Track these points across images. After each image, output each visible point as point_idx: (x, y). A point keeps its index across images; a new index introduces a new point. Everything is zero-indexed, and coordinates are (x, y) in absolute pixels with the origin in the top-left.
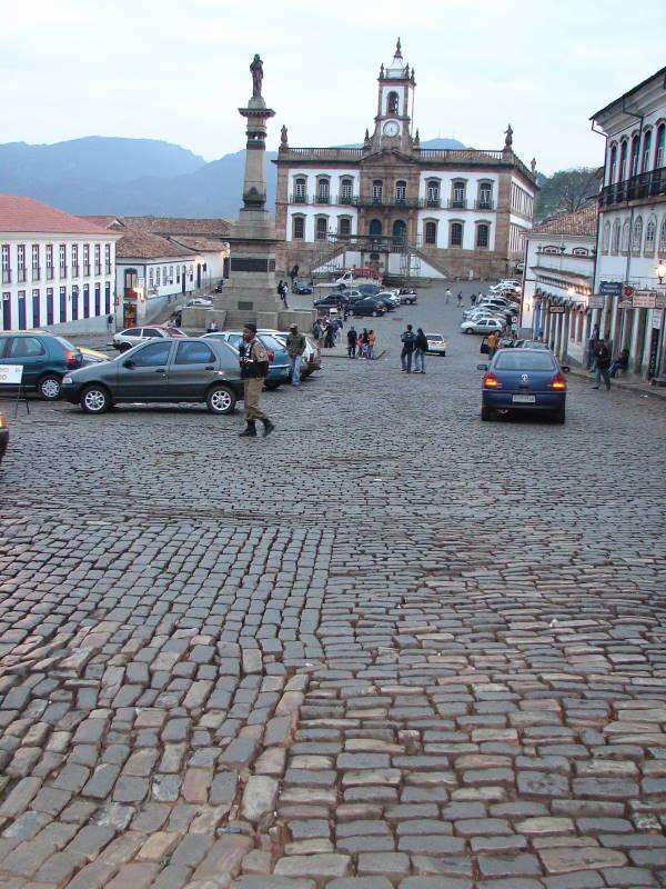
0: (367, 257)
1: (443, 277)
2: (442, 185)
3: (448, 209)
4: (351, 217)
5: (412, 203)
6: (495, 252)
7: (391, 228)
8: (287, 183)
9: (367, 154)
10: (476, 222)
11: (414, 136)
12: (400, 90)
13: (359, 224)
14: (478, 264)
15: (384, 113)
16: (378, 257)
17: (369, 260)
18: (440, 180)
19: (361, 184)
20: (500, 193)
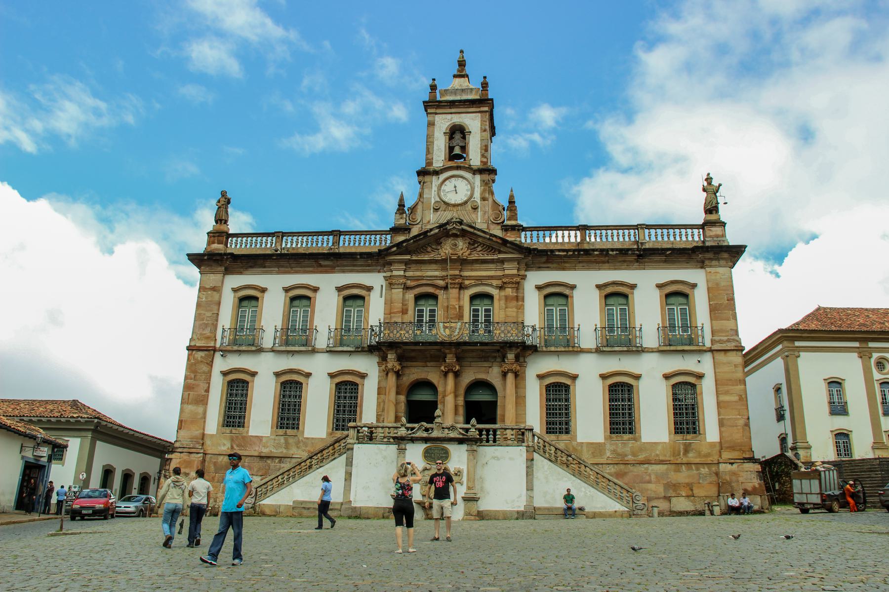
2: (577, 297)
3: (598, 351)
5: (513, 336)
6: (722, 446)
7: (461, 401)
8: (219, 304)
9: (401, 238)
10: (667, 377)
11: (506, 205)
12: (473, 122)
13: (381, 391)
14: (683, 476)
15: (439, 159)
16: (445, 455)
18: (573, 287)
19: (389, 303)
20: (714, 310)
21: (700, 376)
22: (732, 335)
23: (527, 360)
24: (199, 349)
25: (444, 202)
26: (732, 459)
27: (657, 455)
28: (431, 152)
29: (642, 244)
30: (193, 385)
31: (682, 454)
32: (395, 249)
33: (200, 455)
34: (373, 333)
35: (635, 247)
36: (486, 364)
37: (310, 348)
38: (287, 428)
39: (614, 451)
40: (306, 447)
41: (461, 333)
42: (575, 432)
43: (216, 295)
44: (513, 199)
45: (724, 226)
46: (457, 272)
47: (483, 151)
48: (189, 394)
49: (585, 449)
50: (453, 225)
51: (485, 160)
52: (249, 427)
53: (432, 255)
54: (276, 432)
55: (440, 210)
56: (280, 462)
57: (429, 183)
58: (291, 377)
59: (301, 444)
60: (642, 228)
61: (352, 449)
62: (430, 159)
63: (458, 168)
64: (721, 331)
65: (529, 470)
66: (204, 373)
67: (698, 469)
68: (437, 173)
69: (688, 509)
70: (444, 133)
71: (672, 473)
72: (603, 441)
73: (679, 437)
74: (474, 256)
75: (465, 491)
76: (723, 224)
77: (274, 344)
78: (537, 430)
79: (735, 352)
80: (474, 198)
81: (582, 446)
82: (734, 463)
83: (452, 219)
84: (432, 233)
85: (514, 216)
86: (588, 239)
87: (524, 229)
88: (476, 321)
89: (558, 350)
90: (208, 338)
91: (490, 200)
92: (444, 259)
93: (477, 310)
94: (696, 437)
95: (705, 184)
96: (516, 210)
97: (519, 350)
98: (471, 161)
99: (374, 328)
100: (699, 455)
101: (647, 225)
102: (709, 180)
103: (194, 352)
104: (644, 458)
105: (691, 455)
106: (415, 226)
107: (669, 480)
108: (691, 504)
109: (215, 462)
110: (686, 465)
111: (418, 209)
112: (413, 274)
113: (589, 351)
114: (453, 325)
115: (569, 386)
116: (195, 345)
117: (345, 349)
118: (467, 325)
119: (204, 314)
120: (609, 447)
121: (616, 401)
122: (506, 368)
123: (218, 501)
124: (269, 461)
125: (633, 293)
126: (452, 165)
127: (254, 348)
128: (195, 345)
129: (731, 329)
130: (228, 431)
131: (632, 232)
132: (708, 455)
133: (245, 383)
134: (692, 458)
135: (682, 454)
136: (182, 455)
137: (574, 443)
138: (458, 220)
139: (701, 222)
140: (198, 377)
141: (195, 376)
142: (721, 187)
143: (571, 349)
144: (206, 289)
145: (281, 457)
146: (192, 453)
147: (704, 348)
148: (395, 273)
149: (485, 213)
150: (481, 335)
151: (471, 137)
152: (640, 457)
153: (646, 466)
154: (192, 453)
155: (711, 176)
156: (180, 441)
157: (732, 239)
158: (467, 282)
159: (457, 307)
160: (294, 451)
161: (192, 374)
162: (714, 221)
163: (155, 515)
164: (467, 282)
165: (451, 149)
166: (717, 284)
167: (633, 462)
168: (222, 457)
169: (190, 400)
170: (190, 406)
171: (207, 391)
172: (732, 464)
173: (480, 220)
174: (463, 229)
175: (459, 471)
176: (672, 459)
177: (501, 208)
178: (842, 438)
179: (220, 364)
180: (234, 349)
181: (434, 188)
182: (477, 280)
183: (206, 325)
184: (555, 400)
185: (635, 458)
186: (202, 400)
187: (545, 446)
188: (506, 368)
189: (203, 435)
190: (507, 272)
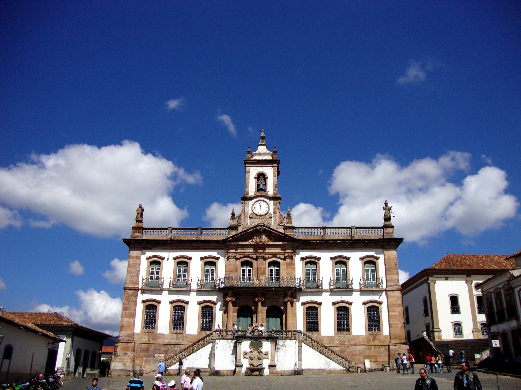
0: (245, 346)
1: (341, 368)
2: (321, 263)
4: (215, 304)
5: (290, 284)
8: (139, 265)
10: (364, 304)
16: (261, 346)
17: (248, 350)
19: (228, 267)
21: (381, 303)
22: (396, 283)
23: (297, 295)
24: (130, 289)
25: (254, 213)
26: (395, 343)
27: (360, 342)
28: (248, 187)
29: (353, 236)
30: (128, 307)
31: (372, 341)
32: (231, 239)
33: (132, 344)
34: (221, 282)
35: (350, 238)
36: (277, 297)
37: (188, 289)
38: (177, 329)
39: (339, 340)
40: (187, 339)
41: (265, 283)
42: (321, 331)
43: (138, 259)
44: (289, 213)
45: (393, 228)
46: (262, 251)
47: (275, 187)
48: (126, 312)
49: (325, 339)
50: (260, 227)
51: (275, 192)
52: (157, 329)
53: (249, 242)
54: (171, 331)
55: (253, 218)
56: (174, 347)
57: (247, 204)
58: (179, 303)
59: (185, 338)
60: (353, 229)
61: (215, 342)
62: (247, 191)
63: (262, 196)
64: (391, 280)
65: (300, 351)
66: (133, 301)
67: (379, 348)
68: (251, 199)
69: (375, 368)
70: (255, 177)
71: (367, 350)
72: (334, 335)
73: (371, 333)
74: (271, 243)
75: (270, 362)
76: (393, 227)
77: (170, 287)
78: (302, 331)
79: (397, 291)
80: (270, 212)
81: (324, 338)
82: (396, 345)
83: (259, 223)
84: (250, 231)
85: (290, 222)
86: (327, 234)
87: (295, 228)
88: (271, 275)
89: (312, 290)
90: (135, 283)
91: (278, 213)
92: (255, 244)
93: (272, 270)
94: (379, 333)
95: (384, 206)
96: (291, 218)
97: (293, 291)
98: (268, 192)
99: (221, 280)
100: (380, 340)
101: (356, 227)
102: (386, 204)
103: (127, 291)
104: (354, 343)
105: (376, 341)
106: (240, 226)
107: (365, 354)
108: (376, 365)
109: (140, 347)
110: (374, 346)
111: (242, 217)
112: (240, 251)
113: (326, 291)
114: (261, 278)
115: (318, 308)
116: (128, 287)
117: (206, 289)
118: (268, 278)
119: (132, 270)
120: (337, 338)
121: (340, 315)
122: (287, 300)
123: (142, 367)
124: (168, 347)
125: (349, 262)
126: (259, 194)
127: (159, 289)
128: (128, 287)
129: (396, 280)
130: (147, 331)
131: (348, 230)
132: (384, 341)
133: (155, 307)
134: (377, 343)
135: (372, 341)
136: (123, 344)
137: (320, 336)
138: (263, 224)
139: (382, 225)
140: (130, 303)
141: (128, 303)
142: (392, 208)
143: (318, 290)
144: (133, 257)
145: (175, 345)
146: (128, 343)
147: (383, 289)
148: (231, 251)
149: (275, 220)
150: (275, 283)
151: (268, 179)
152: (352, 343)
153: (355, 347)
154: (128, 343)
155: (387, 202)
156: (121, 336)
157: (396, 235)
158: (267, 256)
159: (262, 268)
160: (181, 341)
161: (127, 302)
162: (388, 225)
163: (110, 375)
164: (267, 256)
165: (258, 186)
166: (389, 257)
167: (349, 345)
168: (144, 344)
169: (126, 315)
170: (126, 318)
171: (135, 310)
172: (395, 346)
173: (273, 224)
174: (265, 229)
175: (267, 353)
176: (367, 343)
177: (283, 218)
178: (458, 327)
179: (141, 297)
180: (149, 289)
181: (250, 206)
182: (272, 254)
183: (134, 276)
184: (310, 315)
185: (350, 343)
186: (133, 315)
187: (306, 339)
188: (287, 300)
189: (134, 333)
190: (287, 251)
